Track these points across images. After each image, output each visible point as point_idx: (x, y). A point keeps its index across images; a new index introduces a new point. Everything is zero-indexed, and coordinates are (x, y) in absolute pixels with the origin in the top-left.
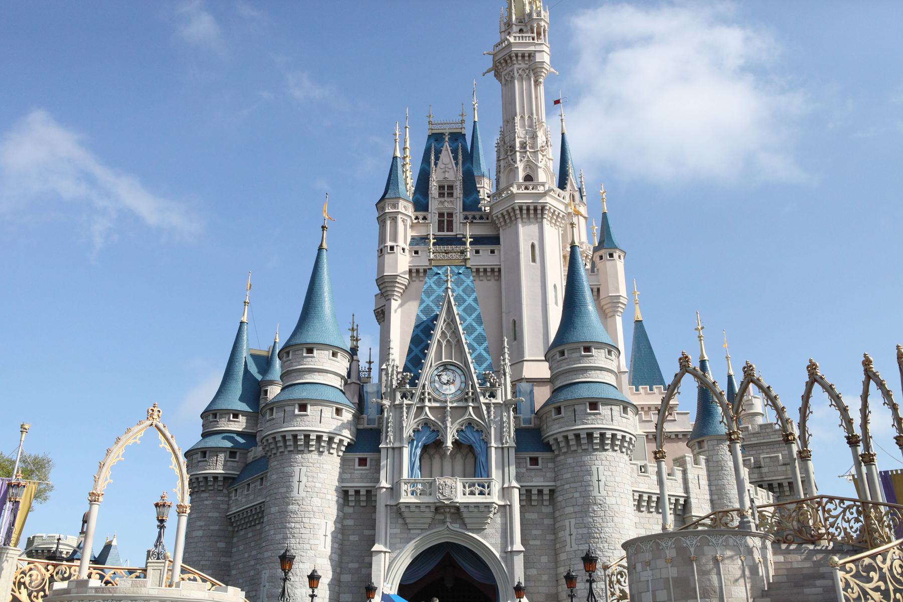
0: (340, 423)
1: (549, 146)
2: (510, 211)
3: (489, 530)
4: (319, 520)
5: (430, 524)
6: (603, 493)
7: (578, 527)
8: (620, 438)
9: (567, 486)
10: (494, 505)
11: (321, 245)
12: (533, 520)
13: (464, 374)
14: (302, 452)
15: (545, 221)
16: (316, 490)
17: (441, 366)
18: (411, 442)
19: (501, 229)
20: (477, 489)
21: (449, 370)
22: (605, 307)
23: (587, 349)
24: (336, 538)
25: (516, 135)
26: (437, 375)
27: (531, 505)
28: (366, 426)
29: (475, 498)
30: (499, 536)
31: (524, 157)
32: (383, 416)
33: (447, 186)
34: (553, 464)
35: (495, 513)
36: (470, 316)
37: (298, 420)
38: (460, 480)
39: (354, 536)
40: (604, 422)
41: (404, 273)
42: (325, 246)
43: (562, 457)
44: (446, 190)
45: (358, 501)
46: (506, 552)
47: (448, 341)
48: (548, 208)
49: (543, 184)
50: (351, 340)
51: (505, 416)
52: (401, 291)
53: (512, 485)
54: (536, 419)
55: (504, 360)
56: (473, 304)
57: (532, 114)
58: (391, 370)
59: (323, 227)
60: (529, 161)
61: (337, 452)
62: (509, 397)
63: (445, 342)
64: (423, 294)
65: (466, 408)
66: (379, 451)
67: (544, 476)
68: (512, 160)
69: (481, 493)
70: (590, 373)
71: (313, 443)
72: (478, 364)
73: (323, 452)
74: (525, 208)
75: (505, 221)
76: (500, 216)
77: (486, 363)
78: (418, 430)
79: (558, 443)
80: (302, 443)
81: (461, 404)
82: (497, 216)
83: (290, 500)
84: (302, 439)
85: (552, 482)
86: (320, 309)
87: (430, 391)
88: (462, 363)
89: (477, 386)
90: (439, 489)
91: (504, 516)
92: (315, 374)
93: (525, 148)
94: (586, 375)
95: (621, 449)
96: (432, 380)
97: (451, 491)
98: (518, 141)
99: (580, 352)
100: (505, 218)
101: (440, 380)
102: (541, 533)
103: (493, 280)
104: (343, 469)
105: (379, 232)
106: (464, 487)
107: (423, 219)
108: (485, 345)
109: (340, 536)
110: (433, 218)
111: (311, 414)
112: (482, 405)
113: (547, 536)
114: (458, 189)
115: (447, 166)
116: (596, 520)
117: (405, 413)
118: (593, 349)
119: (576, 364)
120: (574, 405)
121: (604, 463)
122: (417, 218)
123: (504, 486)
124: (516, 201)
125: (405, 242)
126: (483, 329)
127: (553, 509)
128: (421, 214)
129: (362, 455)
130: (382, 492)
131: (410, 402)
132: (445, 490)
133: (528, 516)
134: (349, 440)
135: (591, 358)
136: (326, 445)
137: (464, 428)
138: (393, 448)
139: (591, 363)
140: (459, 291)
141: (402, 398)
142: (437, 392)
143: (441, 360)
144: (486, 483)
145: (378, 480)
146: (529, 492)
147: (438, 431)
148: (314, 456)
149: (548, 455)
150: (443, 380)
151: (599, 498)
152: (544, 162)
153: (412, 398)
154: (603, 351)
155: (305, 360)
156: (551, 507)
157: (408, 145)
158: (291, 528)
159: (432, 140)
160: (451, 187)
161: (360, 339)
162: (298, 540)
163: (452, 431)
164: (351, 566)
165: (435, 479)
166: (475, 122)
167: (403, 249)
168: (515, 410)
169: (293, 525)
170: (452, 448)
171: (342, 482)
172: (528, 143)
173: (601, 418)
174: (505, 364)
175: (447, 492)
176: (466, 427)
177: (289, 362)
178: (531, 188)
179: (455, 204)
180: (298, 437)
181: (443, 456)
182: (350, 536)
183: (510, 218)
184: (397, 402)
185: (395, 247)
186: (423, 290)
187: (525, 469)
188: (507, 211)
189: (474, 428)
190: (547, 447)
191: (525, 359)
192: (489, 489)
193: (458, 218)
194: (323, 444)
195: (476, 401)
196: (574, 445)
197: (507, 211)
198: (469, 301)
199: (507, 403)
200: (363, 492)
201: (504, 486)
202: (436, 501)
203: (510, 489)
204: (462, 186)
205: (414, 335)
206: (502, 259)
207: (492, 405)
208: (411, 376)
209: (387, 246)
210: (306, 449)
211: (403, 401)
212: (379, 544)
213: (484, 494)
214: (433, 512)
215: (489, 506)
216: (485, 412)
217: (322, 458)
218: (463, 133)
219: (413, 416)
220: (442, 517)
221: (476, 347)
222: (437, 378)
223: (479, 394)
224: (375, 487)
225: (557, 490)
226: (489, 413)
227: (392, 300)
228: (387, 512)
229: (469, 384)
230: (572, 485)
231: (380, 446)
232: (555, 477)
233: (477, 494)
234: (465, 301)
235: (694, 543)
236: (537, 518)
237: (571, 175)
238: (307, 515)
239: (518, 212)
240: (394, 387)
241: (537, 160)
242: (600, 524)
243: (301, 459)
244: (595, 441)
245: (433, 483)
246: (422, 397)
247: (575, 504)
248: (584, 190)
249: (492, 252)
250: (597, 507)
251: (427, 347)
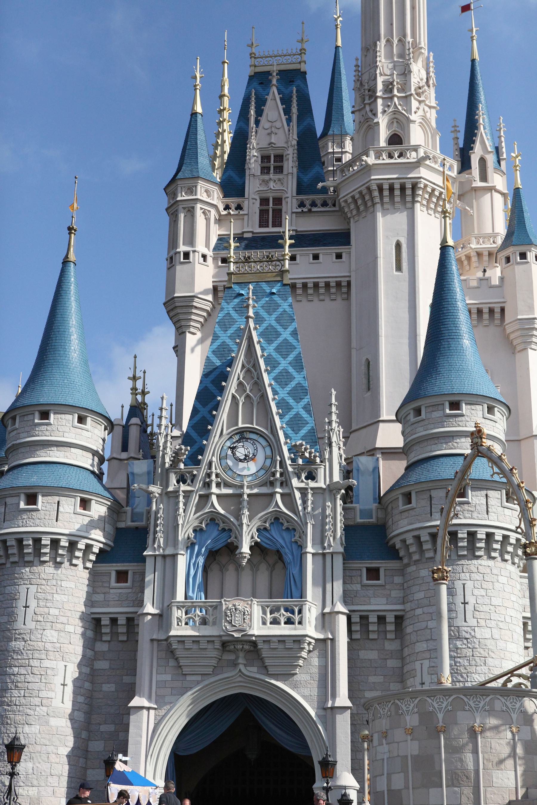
0: (86, 520)
1: (431, 85)
2: (364, 192)
3: (301, 676)
4: (55, 662)
5: (215, 667)
6: (472, 622)
7: (433, 672)
8: (501, 539)
9: (419, 611)
10: (307, 638)
11: (67, 256)
12: (370, 660)
13: (270, 445)
14: (30, 564)
15: (417, 206)
16: (51, 618)
17: (236, 434)
18: (190, 546)
19: (352, 220)
20: (283, 615)
21: (247, 439)
22: (512, 336)
23: (455, 405)
24: (80, 688)
25: (378, 72)
26: (230, 447)
27: (368, 639)
28: (130, 524)
29: (280, 629)
30: (315, 684)
31: (389, 106)
32: (151, 508)
33: (274, 156)
34: (401, 577)
35: (309, 651)
36: (284, 358)
37: (23, 517)
38: (257, 602)
39: (109, 685)
40: (475, 515)
41: (205, 292)
42: (72, 257)
43: (413, 568)
45: (114, 634)
46: (325, 709)
47: (248, 396)
48: (422, 186)
49: (415, 149)
50: (131, 393)
51: (329, 507)
52: (202, 320)
53: (336, 610)
54: (379, 510)
55: (330, 423)
56: (291, 339)
57: (405, 36)
58: (163, 440)
59: (70, 229)
60: (396, 112)
61: (84, 563)
63: (243, 398)
64: (217, 326)
65: (272, 495)
66: (143, 560)
67: (388, 596)
68: (371, 111)
69: (289, 622)
70: (458, 440)
71: (47, 550)
72: (293, 430)
73: (61, 563)
74: (386, 187)
75: (358, 208)
76: (350, 200)
77: (305, 428)
78: (201, 530)
79: (407, 547)
80: (30, 551)
81: (265, 490)
82: (346, 201)
83: (12, 634)
84: (30, 545)
85: (399, 604)
86: (62, 352)
87: (218, 471)
88: (267, 430)
89: (289, 462)
90: (226, 615)
91: (323, 656)
92: (52, 449)
93: (391, 91)
94: (452, 445)
95: (502, 555)
96: (223, 454)
97: (244, 619)
98: (380, 80)
99: (444, 410)
100: (357, 203)
101: (234, 454)
102: (382, 680)
103: (339, 298)
104: (93, 587)
105: (169, 231)
106: (264, 613)
107: (236, 209)
108: (305, 401)
109: (87, 685)
111: (44, 508)
112: (295, 491)
113: (391, 684)
114: (291, 159)
115: (274, 124)
116: (459, 662)
117: (181, 505)
118: (464, 405)
119: (438, 428)
120: (430, 490)
121: (475, 576)
122: (227, 208)
123: (324, 611)
124: (373, 177)
125: (207, 245)
126: (304, 377)
127: (402, 645)
128: (233, 201)
129: (121, 567)
130: (145, 621)
131: (189, 488)
132: (235, 617)
133: (365, 655)
134: (101, 546)
135: (460, 419)
136: (66, 553)
137: (267, 525)
138: (164, 557)
139: (459, 426)
140: (271, 320)
141: (178, 482)
142: (230, 473)
143: (237, 424)
144: (296, 606)
145: (141, 603)
147: (230, 530)
148: (49, 569)
149: (393, 564)
150: (238, 454)
151: (465, 629)
152: (420, 112)
153: (192, 482)
154: (479, 407)
155: (37, 429)
156: (398, 642)
157: (226, 91)
158: (14, 675)
159: (255, 84)
160: (279, 158)
161: (148, 392)
162: (22, 692)
163: (250, 530)
164: (103, 728)
165: (221, 602)
166: (337, 47)
167: (204, 257)
168: (345, 499)
169: (16, 670)
170: (250, 555)
171: (92, 606)
172: (395, 83)
173: (470, 509)
174: (332, 430)
175: (237, 620)
176: (271, 524)
177: (15, 432)
178: (396, 155)
179: (285, 184)
180: (25, 543)
181: (239, 567)
182: (103, 685)
183: (365, 203)
184: (171, 489)
185: (191, 254)
186: (217, 320)
187: (358, 587)
188: (360, 193)
189: (282, 524)
191: (380, 419)
192: (300, 615)
194: (60, 552)
195: (287, 485)
196: (430, 549)
197: (360, 193)
198: (285, 336)
199: (332, 488)
200: (122, 621)
201: (324, 611)
202: (222, 633)
203: (333, 615)
204: (295, 155)
205: (201, 388)
206: (353, 267)
207: (309, 490)
208: (186, 450)
209: (179, 253)
210: (37, 559)
211: (179, 487)
212: (140, 697)
213: (293, 623)
214: (218, 649)
215: (299, 641)
216: (299, 502)
217: (59, 572)
218: (302, 70)
219: (194, 509)
220: (232, 657)
221: (291, 404)
222: (230, 452)
223: (291, 475)
224: (137, 612)
225: (406, 617)
226: (304, 502)
227: (188, 334)
228: (153, 648)
229: (277, 460)
230: (426, 610)
231: (145, 553)
232: (404, 597)
233: (282, 623)
234: (278, 335)
235: (444, 706)
236: (376, 657)
237: (482, 127)
238: (36, 655)
239: (376, 194)
240: (167, 465)
241: (409, 111)
242: (465, 669)
243: (28, 574)
244: (460, 544)
245: (218, 607)
246: (208, 480)
247: (430, 638)
248: (504, 150)
249: (339, 256)
250: (461, 643)
251: (217, 406)
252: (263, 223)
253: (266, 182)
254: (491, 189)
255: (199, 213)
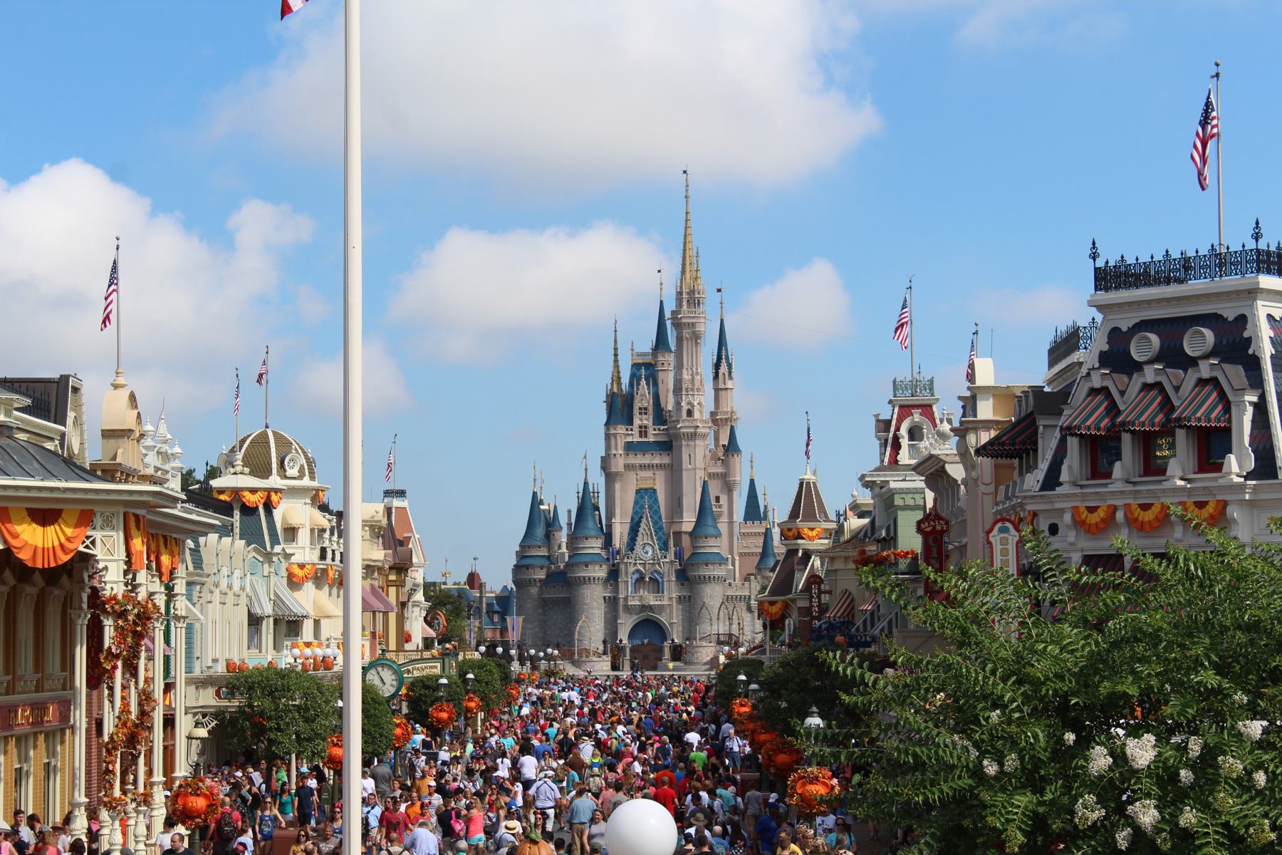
3: (663, 614)
20: (658, 598)
44: (644, 411)
45: (610, 601)
62: (673, 559)
110: (636, 431)
122: (627, 430)
146: (680, 597)
190: (688, 579)
193: (651, 431)
251: (637, 536)
252: (641, 436)
253: (641, 420)
254: (726, 389)
255: (618, 437)
